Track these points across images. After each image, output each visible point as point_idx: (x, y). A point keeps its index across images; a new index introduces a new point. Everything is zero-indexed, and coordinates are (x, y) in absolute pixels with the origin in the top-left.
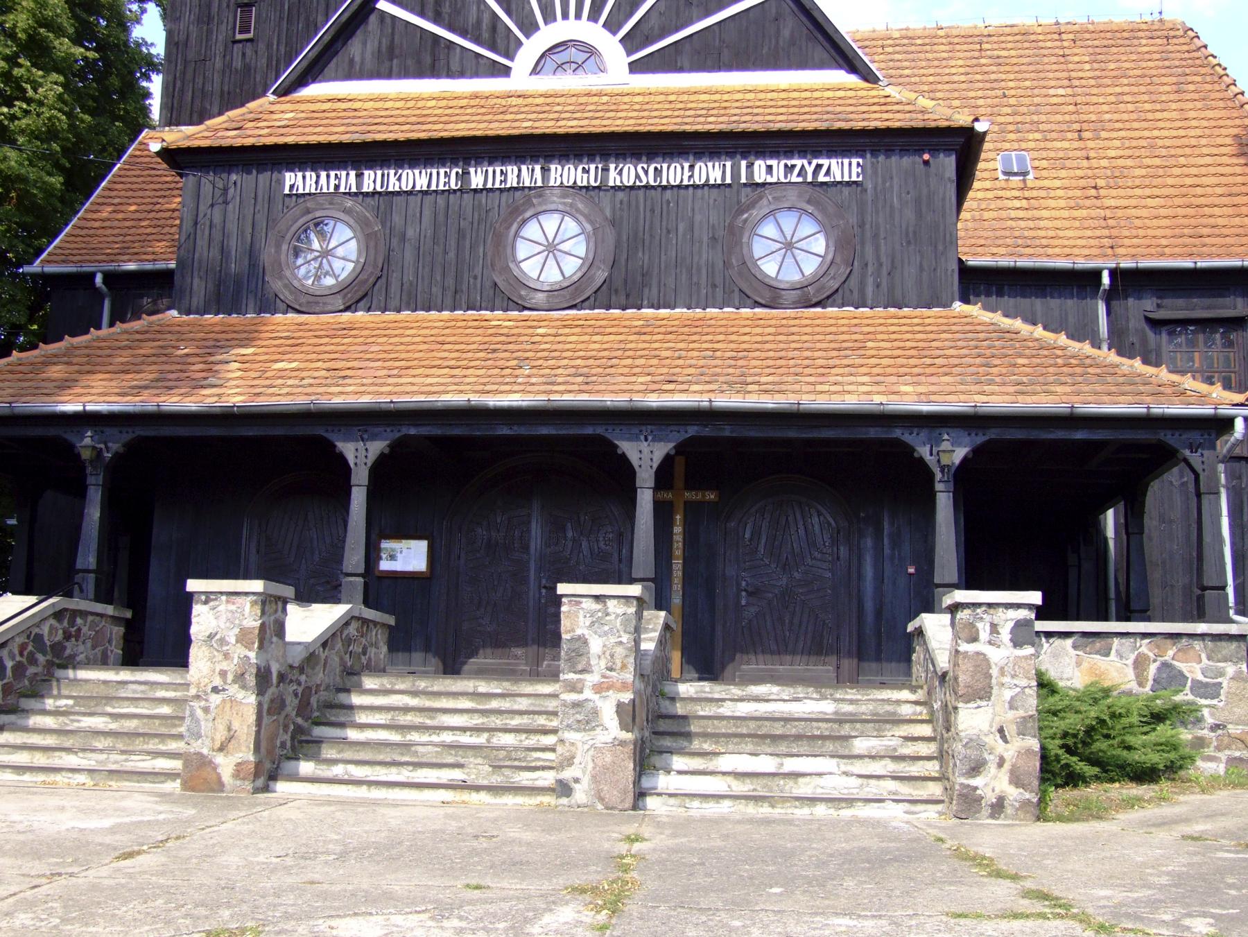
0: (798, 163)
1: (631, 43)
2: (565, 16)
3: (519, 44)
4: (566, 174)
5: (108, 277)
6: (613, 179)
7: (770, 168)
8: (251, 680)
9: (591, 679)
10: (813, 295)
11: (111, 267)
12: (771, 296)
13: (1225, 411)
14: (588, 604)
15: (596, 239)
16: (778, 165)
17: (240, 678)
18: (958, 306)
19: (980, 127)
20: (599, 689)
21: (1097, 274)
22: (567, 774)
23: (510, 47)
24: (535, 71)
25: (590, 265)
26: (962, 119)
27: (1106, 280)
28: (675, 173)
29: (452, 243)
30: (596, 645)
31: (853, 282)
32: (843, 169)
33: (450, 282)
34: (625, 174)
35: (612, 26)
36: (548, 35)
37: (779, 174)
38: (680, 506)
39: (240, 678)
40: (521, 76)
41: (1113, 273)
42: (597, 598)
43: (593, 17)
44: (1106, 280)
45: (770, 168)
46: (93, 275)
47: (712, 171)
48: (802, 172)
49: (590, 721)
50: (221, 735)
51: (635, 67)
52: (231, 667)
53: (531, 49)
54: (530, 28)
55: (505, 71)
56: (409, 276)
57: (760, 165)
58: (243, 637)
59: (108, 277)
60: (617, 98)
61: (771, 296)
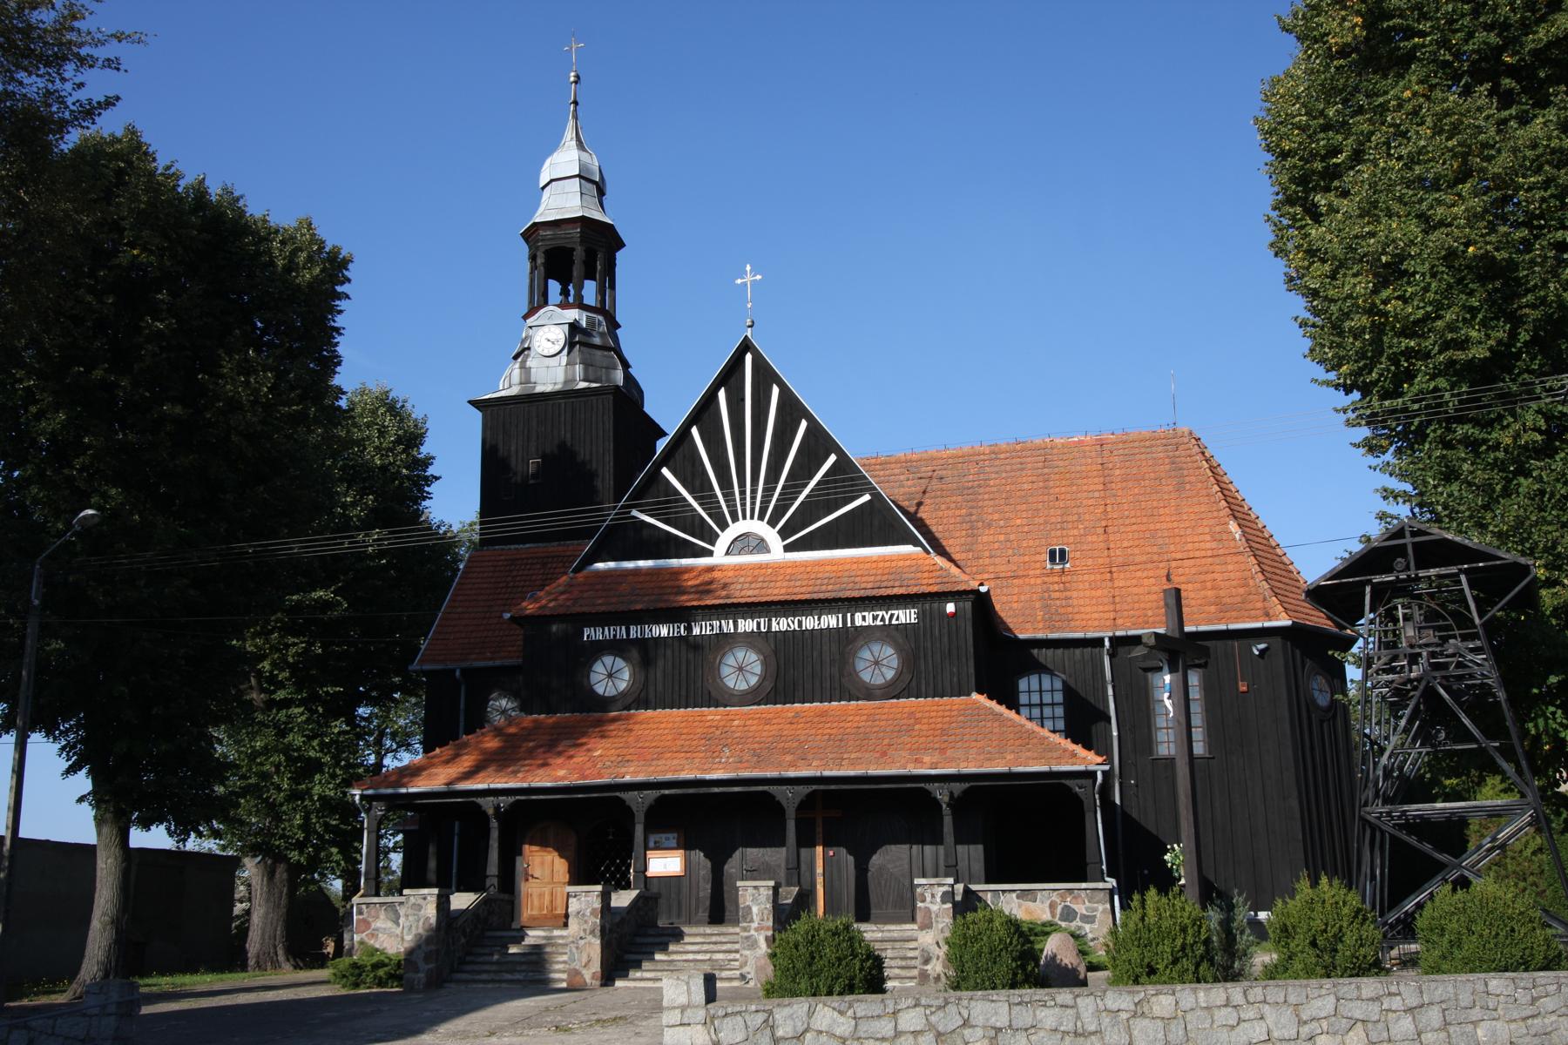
0: (880, 613)
1: (784, 534)
2: (744, 517)
3: (717, 536)
4: (747, 625)
5: (463, 671)
6: (775, 627)
7: (864, 618)
8: (598, 933)
9: (754, 925)
10: (894, 690)
11: (465, 665)
12: (868, 693)
13: (1092, 768)
14: (750, 890)
15: (765, 664)
16: (869, 616)
17: (592, 932)
18: (975, 696)
20: (757, 930)
21: (1100, 641)
22: (744, 970)
23: (712, 538)
24: (727, 553)
25: (763, 678)
27: (1107, 643)
28: (810, 623)
29: (684, 668)
30: (755, 909)
31: (914, 683)
32: (906, 616)
33: (683, 693)
34: (782, 624)
35: (772, 523)
36: (735, 529)
37: (869, 621)
38: (819, 822)
39: (592, 932)
40: (719, 555)
41: (1111, 639)
42: (756, 887)
43: (761, 518)
44: (1107, 643)
45: (864, 618)
46: (454, 671)
47: (831, 621)
48: (883, 619)
49: (753, 945)
50: (584, 960)
51: (787, 548)
52: (588, 927)
53: (725, 538)
54: (723, 526)
55: (710, 553)
56: (660, 688)
57: (858, 616)
58: (593, 912)
59: (463, 671)
60: (777, 568)
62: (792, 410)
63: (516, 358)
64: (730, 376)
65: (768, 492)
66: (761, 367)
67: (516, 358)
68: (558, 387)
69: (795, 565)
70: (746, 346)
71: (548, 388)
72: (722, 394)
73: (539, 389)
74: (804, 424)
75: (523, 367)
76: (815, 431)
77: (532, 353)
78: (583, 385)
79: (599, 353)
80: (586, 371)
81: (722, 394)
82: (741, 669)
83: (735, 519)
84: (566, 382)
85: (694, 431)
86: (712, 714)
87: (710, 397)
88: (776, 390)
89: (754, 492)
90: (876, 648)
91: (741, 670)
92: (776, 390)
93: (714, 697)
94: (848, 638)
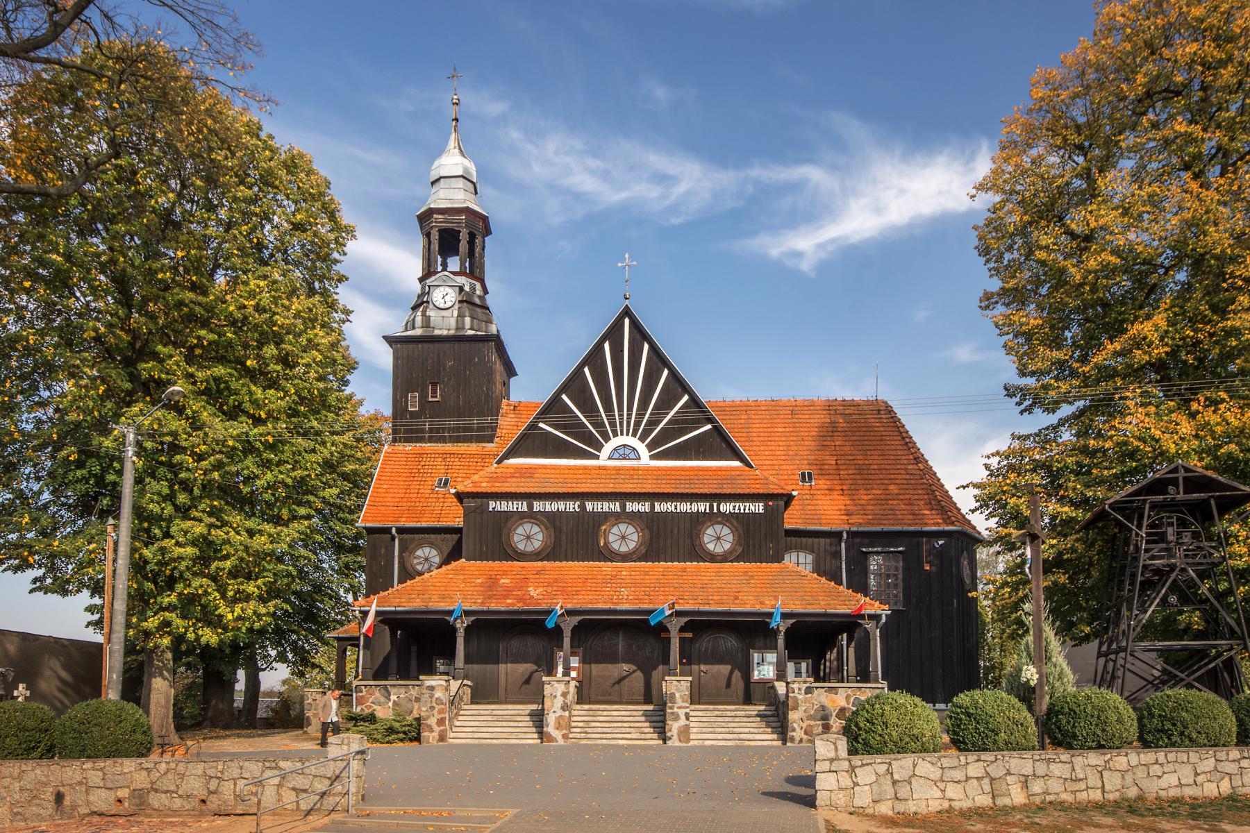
1: (651, 447)
12: (713, 558)
19: (794, 493)
23: (599, 447)
26: (787, 489)
35: (642, 439)
40: (604, 458)
43: (634, 435)
51: (652, 457)
53: (608, 448)
54: (607, 439)
55: (597, 457)
61: (713, 558)
62: (659, 360)
63: (415, 308)
64: (614, 333)
65: (640, 416)
66: (635, 325)
67: (415, 308)
68: (452, 332)
69: (659, 469)
70: (627, 312)
71: (445, 333)
72: (607, 346)
73: (437, 332)
74: (666, 372)
75: (424, 314)
76: (674, 374)
77: (431, 306)
78: (472, 332)
79: (479, 310)
80: (472, 322)
81: (607, 346)
82: (623, 537)
83: (615, 435)
84: (457, 329)
85: (586, 370)
86: (607, 567)
87: (599, 347)
88: (646, 346)
89: (629, 415)
90: (718, 527)
91: (624, 537)
92: (646, 346)
93: (608, 555)
94: (699, 521)
